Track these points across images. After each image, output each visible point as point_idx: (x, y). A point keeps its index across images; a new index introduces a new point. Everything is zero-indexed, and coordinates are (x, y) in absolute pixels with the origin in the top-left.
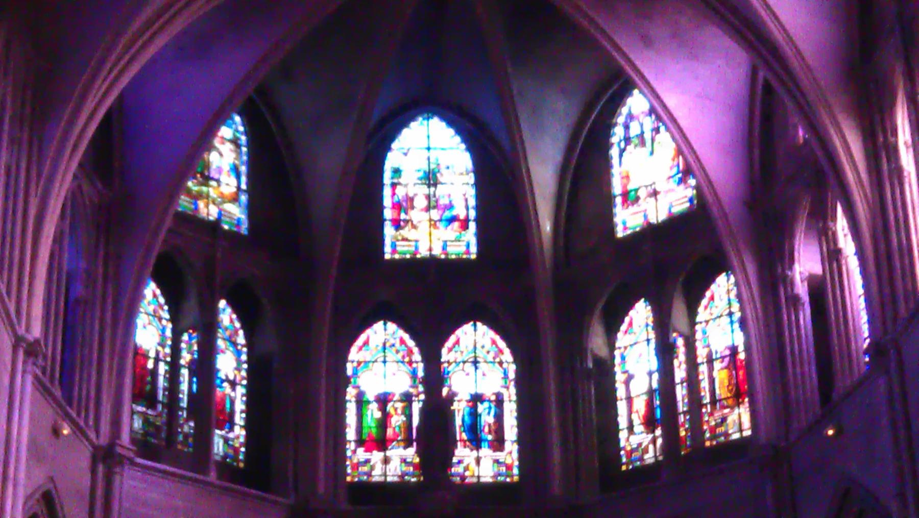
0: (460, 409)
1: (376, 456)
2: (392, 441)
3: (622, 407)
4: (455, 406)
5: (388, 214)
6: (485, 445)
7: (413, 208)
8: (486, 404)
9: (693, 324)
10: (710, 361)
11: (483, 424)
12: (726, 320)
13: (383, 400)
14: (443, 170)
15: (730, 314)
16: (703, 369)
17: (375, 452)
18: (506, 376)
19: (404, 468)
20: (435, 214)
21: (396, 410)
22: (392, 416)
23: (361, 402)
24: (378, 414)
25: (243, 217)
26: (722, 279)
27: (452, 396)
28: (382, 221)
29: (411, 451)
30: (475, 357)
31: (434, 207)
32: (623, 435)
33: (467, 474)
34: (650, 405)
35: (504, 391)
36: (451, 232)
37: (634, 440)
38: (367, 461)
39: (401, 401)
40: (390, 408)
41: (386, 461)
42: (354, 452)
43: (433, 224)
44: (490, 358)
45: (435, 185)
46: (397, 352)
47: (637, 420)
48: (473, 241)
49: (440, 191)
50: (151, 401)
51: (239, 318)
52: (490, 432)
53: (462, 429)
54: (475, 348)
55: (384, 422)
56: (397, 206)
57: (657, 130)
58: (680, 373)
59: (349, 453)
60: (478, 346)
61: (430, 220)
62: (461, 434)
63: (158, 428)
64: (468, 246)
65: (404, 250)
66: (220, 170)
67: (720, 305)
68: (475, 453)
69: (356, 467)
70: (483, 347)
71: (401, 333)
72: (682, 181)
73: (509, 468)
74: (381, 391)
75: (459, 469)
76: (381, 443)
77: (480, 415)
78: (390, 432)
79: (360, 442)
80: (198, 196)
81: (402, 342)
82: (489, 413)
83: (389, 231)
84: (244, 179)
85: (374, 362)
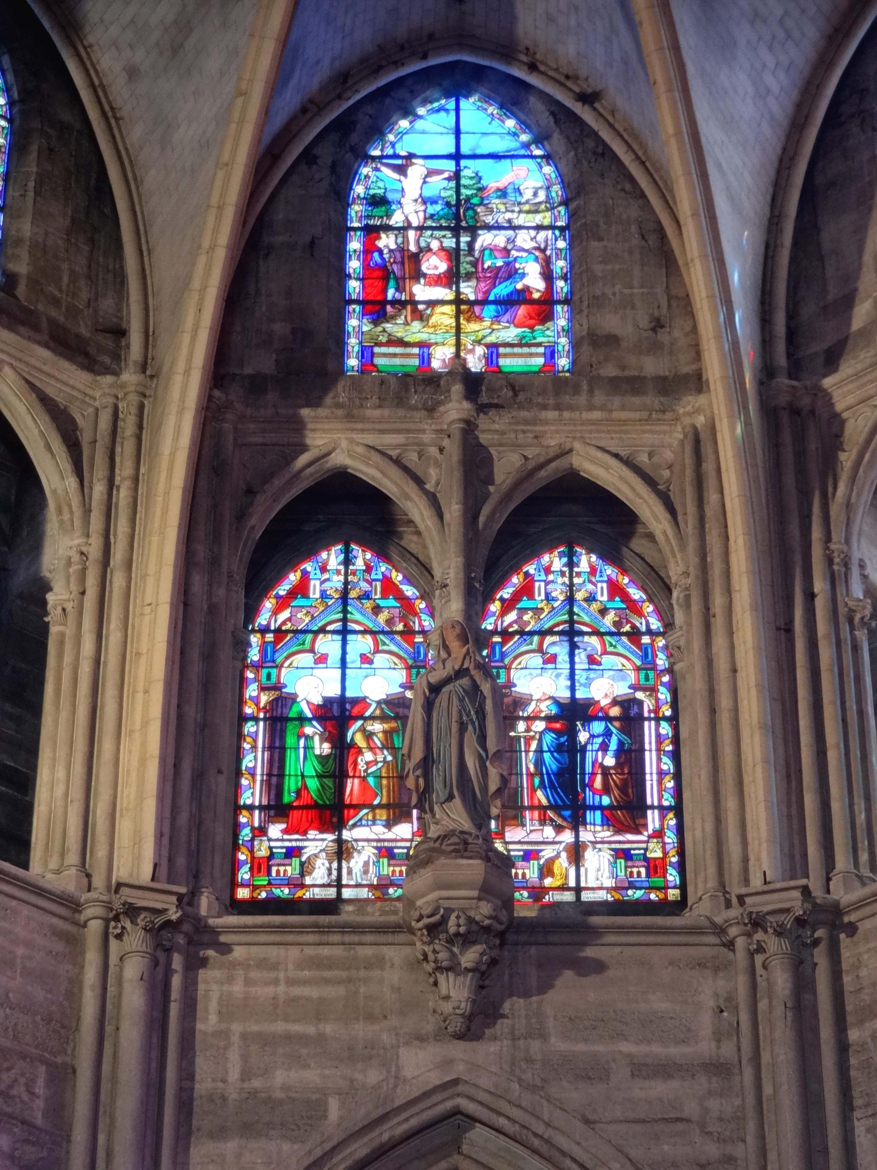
2: (357, 807)
5: (354, 287)
7: (417, 275)
8: (598, 727)
11: (589, 768)
14: (495, 203)
17: (312, 834)
18: (648, 664)
19: (386, 869)
20: (468, 290)
21: (369, 736)
22: (360, 751)
30: (571, 622)
31: (468, 276)
33: (548, 882)
35: (640, 695)
38: (292, 853)
39: (383, 718)
42: (261, 831)
44: (608, 621)
45: (473, 231)
46: (377, 610)
49: (485, 239)
52: (606, 789)
53: (537, 781)
54: (570, 600)
59: (246, 834)
60: (579, 596)
61: (458, 301)
62: (533, 790)
64: (551, 353)
68: (567, 837)
69: (260, 866)
70: (591, 599)
73: (655, 867)
74: (333, 690)
75: (531, 872)
77: (584, 750)
78: (352, 786)
81: (389, 587)
82: (604, 747)
85: (316, 633)
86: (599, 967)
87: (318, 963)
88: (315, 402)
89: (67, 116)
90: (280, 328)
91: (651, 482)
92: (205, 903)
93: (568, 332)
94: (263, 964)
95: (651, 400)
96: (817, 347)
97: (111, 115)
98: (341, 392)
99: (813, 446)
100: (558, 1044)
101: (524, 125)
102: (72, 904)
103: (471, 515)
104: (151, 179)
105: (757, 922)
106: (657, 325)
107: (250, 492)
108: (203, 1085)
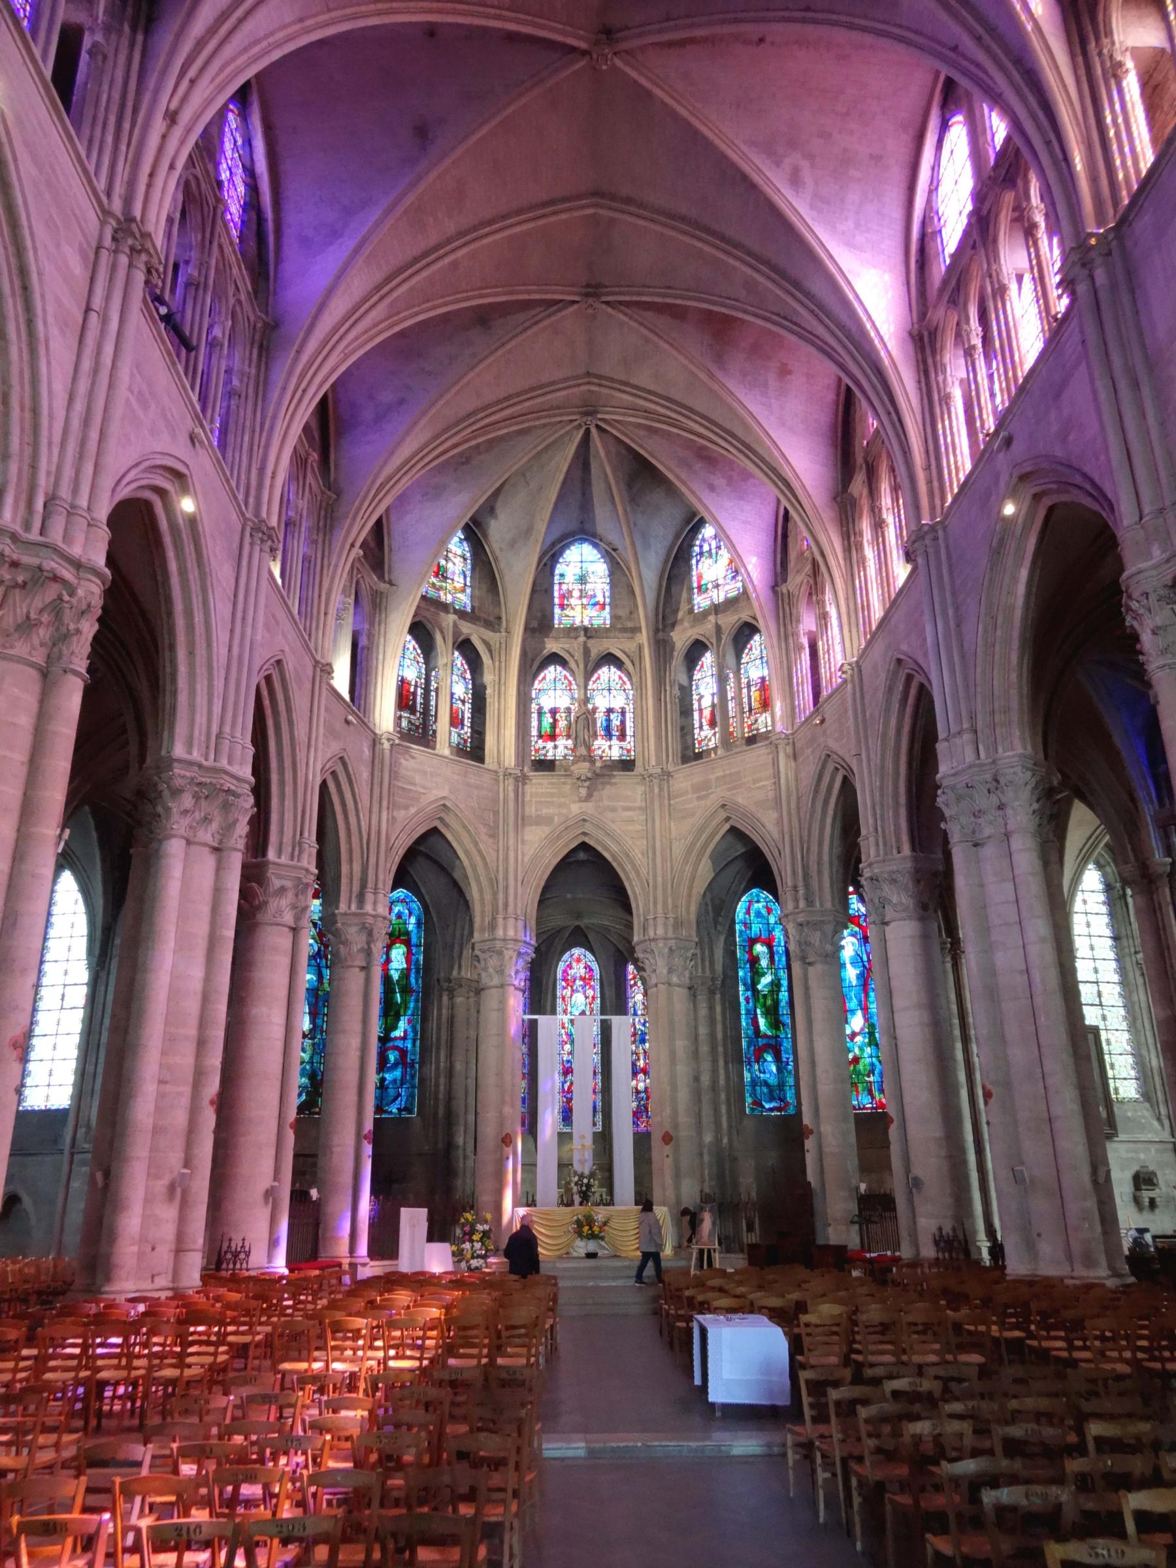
0: (600, 717)
1: (550, 745)
3: (696, 715)
4: (597, 715)
5: (557, 601)
6: (614, 738)
9: (739, 663)
10: (749, 686)
12: (758, 662)
13: (554, 712)
15: (762, 658)
16: (745, 691)
18: (628, 698)
20: (585, 601)
23: (540, 713)
24: (551, 720)
25: (468, 602)
26: (757, 637)
27: (595, 710)
28: (553, 605)
29: (570, 743)
32: (696, 731)
34: (713, 714)
36: (592, 612)
37: (703, 734)
40: (558, 716)
41: (556, 747)
43: (584, 606)
44: (618, 687)
47: (705, 722)
48: (608, 617)
49: (588, 586)
50: (413, 711)
51: (468, 663)
55: (554, 725)
56: (562, 597)
57: (719, 548)
58: (730, 695)
63: (418, 727)
65: (567, 622)
66: (454, 573)
67: (756, 652)
69: (537, 751)
71: (564, 672)
72: (734, 578)
73: (629, 751)
75: (600, 752)
76: (553, 737)
78: (558, 731)
79: (540, 736)
80: (439, 589)
81: (566, 677)
83: (557, 610)
84: (468, 579)
86: (615, 784)
87: (552, 784)
88: (548, 637)
89: (484, 558)
90: (539, 615)
91: (628, 656)
92: (526, 769)
93: (610, 613)
94: (540, 784)
95: (629, 635)
96: (669, 622)
97: (496, 559)
98: (553, 633)
99: (668, 649)
100: (606, 803)
101: (599, 551)
102: (496, 772)
103: (586, 666)
104: (506, 578)
105: (651, 775)
106: (631, 613)
107: (533, 660)
108: (527, 813)
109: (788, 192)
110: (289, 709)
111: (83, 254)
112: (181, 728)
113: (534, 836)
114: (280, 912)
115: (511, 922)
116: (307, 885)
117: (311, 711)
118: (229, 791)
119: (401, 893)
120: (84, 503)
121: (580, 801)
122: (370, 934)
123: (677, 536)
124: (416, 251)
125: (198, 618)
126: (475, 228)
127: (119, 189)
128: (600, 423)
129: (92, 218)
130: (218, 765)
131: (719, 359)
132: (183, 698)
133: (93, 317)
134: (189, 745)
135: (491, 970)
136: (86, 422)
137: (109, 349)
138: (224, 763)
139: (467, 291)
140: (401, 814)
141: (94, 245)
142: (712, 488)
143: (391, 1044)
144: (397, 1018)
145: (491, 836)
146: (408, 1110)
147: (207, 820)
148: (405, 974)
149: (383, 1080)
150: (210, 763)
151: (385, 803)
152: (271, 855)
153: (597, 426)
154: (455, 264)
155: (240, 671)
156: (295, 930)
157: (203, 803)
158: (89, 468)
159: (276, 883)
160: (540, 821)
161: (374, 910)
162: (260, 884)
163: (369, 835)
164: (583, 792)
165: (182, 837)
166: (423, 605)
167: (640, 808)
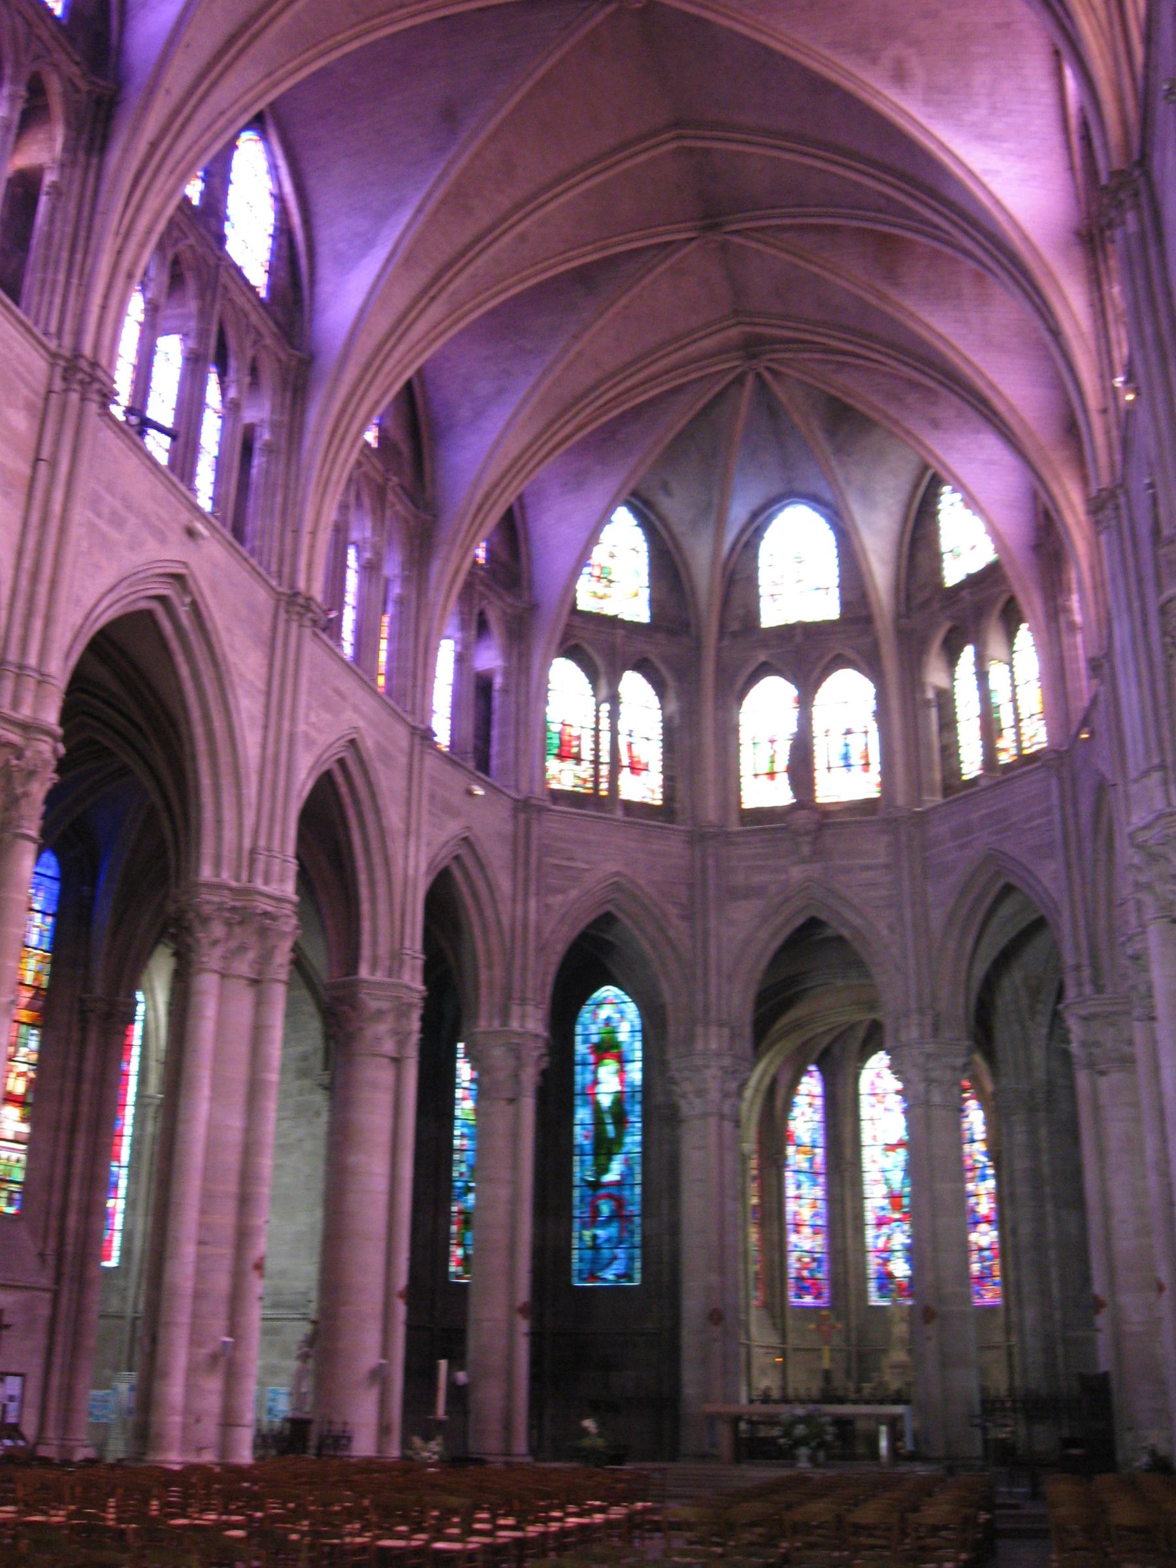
50: (578, 759)
63: (585, 781)
109: (892, 94)
110: (373, 796)
111: (29, 407)
112: (208, 848)
113: (744, 913)
114: (378, 1039)
115: (714, 1030)
116: (410, 1006)
117: (409, 789)
118: (266, 914)
119: (608, 991)
120: (32, 661)
121: (802, 861)
122: (518, 1058)
123: (916, 486)
124: (466, 238)
125: (218, 723)
126: (534, 196)
127: (69, 326)
128: (774, 366)
129: (39, 364)
130: (251, 885)
131: (891, 275)
132: (208, 815)
133: (43, 468)
134: (218, 864)
135: (691, 1096)
136: (35, 577)
137: (58, 495)
138: (259, 884)
139: (547, 259)
140: (556, 900)
141: (42, 390)
142: (935, 424)
143: (603, 1192)
144: (609, 1156)
145: (683, 917)
146: (628, 1276)
147: (243, 948)
148: (619, 1100)
149: (595, 1237)
150: (244, 882)
151: (533, 888)
152: (364, 972)
153: (768, 369)
154: (522, 238)
155: (276, 774)
156: (397, 1061)
157: (237, 930)
158: (38, 624)
159: (373, 1005)
160: (750, 892)
161: (522, 1026)
162: (354, 1007)
163: (513, 930)
164: (806, 850)
165: (216, 972)
166: (577, 622)
167: (886, 866)
